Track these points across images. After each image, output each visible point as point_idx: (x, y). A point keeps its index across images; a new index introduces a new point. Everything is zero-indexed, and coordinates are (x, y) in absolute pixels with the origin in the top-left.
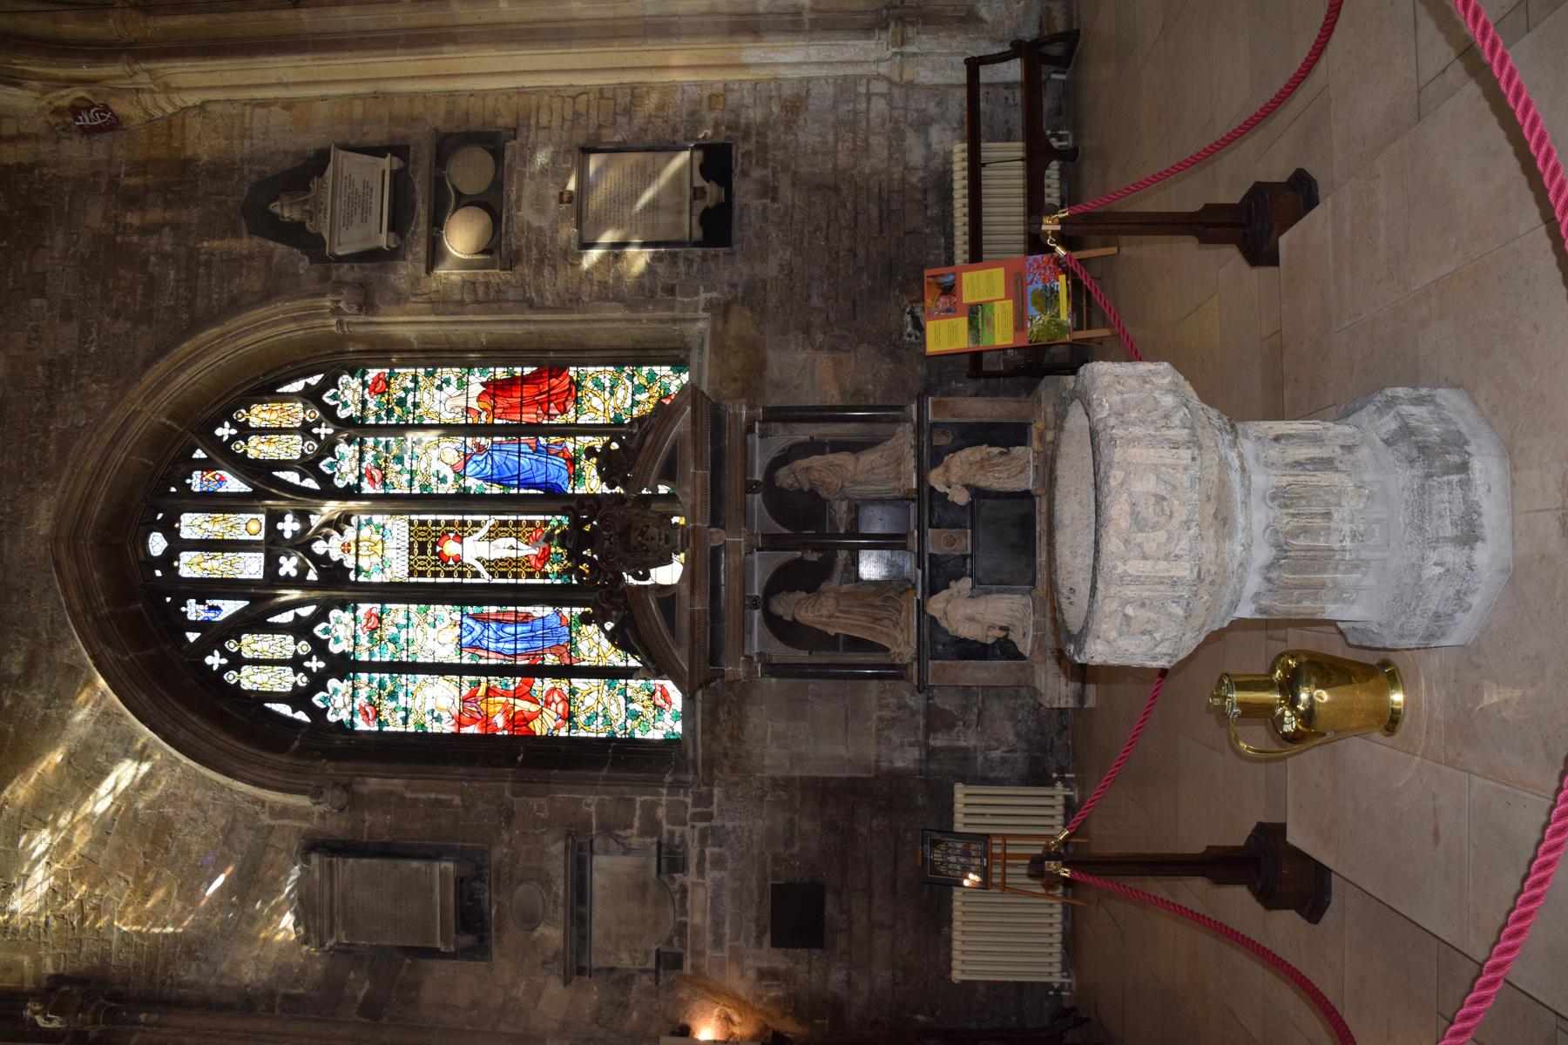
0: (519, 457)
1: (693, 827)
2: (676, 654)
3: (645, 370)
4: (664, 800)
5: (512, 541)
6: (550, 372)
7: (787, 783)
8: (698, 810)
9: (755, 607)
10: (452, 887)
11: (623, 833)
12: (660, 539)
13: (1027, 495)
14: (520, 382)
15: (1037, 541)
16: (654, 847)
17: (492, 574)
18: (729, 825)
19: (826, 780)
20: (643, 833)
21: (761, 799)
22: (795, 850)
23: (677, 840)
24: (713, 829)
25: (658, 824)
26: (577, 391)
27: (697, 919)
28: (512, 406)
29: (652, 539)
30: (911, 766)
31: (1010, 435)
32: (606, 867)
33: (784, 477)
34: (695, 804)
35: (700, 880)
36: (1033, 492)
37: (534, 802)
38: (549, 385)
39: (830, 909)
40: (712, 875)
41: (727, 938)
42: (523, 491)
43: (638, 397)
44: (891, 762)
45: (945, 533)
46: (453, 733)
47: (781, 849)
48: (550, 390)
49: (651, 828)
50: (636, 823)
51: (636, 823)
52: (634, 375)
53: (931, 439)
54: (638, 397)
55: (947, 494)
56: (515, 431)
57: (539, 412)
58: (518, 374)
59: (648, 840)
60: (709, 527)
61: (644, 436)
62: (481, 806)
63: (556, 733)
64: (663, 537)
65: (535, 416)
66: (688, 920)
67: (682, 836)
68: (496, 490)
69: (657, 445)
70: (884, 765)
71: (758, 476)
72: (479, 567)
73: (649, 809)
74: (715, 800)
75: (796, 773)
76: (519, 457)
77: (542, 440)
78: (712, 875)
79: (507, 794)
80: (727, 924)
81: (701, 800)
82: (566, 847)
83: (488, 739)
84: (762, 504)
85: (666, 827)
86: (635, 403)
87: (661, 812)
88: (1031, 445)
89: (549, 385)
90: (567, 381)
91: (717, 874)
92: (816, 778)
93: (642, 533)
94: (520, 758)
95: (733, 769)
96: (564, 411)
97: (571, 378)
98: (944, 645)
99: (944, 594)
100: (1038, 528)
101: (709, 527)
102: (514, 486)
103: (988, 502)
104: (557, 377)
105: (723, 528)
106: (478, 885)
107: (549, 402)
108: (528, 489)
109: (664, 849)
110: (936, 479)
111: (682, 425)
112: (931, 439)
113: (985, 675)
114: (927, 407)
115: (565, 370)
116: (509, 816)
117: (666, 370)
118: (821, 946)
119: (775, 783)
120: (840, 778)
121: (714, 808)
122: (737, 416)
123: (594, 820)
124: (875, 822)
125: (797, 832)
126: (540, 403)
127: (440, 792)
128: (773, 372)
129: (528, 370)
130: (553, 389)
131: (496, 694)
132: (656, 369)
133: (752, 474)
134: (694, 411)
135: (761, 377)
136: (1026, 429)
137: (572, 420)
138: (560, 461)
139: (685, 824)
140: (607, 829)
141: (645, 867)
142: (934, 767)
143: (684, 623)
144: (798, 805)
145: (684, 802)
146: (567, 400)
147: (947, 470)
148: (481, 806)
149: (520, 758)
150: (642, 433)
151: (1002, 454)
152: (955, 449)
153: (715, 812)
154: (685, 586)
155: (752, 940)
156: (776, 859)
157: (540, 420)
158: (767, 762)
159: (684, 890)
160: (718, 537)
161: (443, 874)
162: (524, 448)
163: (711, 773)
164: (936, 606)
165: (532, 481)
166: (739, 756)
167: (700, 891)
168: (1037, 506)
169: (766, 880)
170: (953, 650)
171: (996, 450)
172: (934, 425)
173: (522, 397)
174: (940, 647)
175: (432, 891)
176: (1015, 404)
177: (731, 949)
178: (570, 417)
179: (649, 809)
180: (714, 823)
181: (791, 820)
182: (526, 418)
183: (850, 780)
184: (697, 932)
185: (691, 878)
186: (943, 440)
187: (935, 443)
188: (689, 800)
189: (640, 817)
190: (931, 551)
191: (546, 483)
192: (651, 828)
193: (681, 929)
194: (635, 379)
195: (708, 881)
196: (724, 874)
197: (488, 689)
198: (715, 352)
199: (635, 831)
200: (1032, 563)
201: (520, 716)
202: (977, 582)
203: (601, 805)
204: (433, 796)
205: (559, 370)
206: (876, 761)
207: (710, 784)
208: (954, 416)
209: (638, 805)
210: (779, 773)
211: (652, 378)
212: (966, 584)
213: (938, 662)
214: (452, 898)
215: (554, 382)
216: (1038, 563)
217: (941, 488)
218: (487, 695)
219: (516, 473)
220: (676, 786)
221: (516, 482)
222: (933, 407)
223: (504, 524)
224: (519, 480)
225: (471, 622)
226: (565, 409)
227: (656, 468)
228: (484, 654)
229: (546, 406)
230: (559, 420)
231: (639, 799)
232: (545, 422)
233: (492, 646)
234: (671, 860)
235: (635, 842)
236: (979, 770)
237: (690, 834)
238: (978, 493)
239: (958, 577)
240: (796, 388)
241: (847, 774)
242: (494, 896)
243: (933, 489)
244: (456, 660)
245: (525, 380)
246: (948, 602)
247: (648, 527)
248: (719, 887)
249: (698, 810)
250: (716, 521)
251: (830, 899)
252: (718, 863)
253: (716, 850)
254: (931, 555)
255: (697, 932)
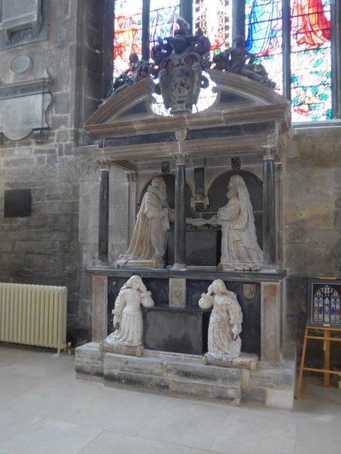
0: (269, 21)
1: (56, 146)
2: (113, 118)
3: (329, 92)
4: (69, 129)
5: (217, 27)
6: (327, 29)
7: (76, 195)
8: (64, 147)
9: (163, 170)
10: (26, 23)
11: (53, 109)
12: (180, 97)
13: (205, 349)
14: (320, 10)
15: (173, 353)
16: (46, 126)
17: (198, 19)
18: (57, 165)
19: (77, 216)
20: (53, 119)
21: (69, 181)
22: (45, 201)
23: (51, 138)
24: (55, 157)
25: (57, 127)
26: (313, 49)
27: (17, 152)
28: (302, 9)
29: (180, 92)
30: (84, 263)
31: (251, 341)
32: (36, 102)
33: (237, 181)
34: (66, 145)
35: (33, 152)
36: (206, 354)
37: (67, 59)
38: (318, 30)
39: (21, 220)
40: (34, 157)
41: (9, 168)
42: (247, 27)
43: (309, 90)
44: (85, 252)
45: (184, 289)
46: (114, 15)
47: (46, 193)
48: (313, 31)
49: (58, 123)
50: (58, 115)
51: (58, 115)
52: (324, 85)
53: (248, 283)
54: (309, 90)
55: (206, 292)
56: (287, 17)
57: (299, 28)
58: (325, 9)
59: (50, 122)
60: (187, 129)
61: (250, 76)
62: (65, 30)
63: (115, 70)
64: (182, 99)
65: (296, 25)
66: (16, 147)
67: (53, 141)
68: (248, 11)
69: (243, 87)
70: (84, 248)
71: (243, 167)
72: (202, 10)
73: (63, 121)
74: (68, 156)
75: (81, 200)
76: (269, 21)
77: (280, 33)
78: (34, 157)
79: (71, 43)
80: (14, 168)
81: (68, 147)
82: (44, 79)
83: (111, 34)
84: (223, 172)
85: (56, 131)
86: (305, 89)
87: (63, 128)
88: (240, 356)
89: (318, 30)
90: (320, 42)
91: (35, 160)
92: (78, 210)
93: (183, 85)
94: (97, 51)
95: (83, 165)
96: (299, 43)
97: (323, 44)
98: (116, 286)
99: (143, 287)
100: (181, 354)
101: (187, 129)
102: (250, 21)
103: (200, 322)
104: (324, 34)
105: (187, 139)
106: (30, 36)
107: (306, 33)
108: (249, 30)
109: (45, 131)
110: (217, 285)
111: (259, 101)
112: (248, 283)
113: (99, 310)
114: (271, 281)
115: (328, 39)
116: (61, 47)
117: (328, 105)
118: (6, 216)
119: (76, 188)
120: (78, 224)
121: (64, 156)
122: (265, 141)
123: (59, 92)
124: (58, 243)
125: (54, 201)
126: (305, 27)
127: (71, 7)
128: (319, 173)
129: (328, 16)
130: (315, 33)
131: (134, 36)
132: (330, 99)
133: (245, 162)
134: (267, 108)
135: (316, 165)
136: (255, 353)
137: (293, 50)
138: (266, 47)
139: (57, 142)
140: (54, 101)
141: (37, 122)
142: (83, 276)
143: (132, 119)
144: (66, 201)
145: (67, 140)
146: (307, 44)
147: (224, 294)
148: (65, 30)
149: (97, 51)
150: (253, 74)
151: (233, 335)
152: (240, 300)
153: (63, 157)
154: (152, 117)
155: (7, 181)
156: (42, 191)
157: (293, 29)
158: (86, 183)
159: (29, 144)
160: (180, 135)
161: (31, 17)
162: (274, 23)
163: (81, 153)
164: (135, 281)
165: (253, 31)
166: (89, 168)
167: (28, 153)
168: (197, 356)
169: (33, 186)
170: (113, 291)
171: (236, 330)
172: (258, 285)
173: (309, 14)
174: (114, 283)
175: (25, 12)
176: (274, 346)
177: (5, 171)
178: (295, 47)
179: (63, 121)
180: (58, 158)
181: (59, 198)
182: (294, 21)
183: (78, 229)
184: (11, 152)
185: (35, 147)
186: (247, 291)
187: (245, 285)
188: (68, 142)
189: (61, 117)
190: (171, 280)
191: (252, 40)
192: (58, 123)
193: (13, 143)
194: (323, 86)
195: (32, 156)
196: (36, 163)
197: (136, 30)
198: (333, 132)
199: (54, 115)
200: (159, 348)
201: (122, 48)
202: (150, 310)
203: (67, 95)
204: (70, 4)
205: (328, 34)
206: (86, 244)
207: (76, 154)
208: (265, 301)
209: (65, 115)
210: (81, 190)
211: (322, 97)
212: (148, 302)
213: (106, 281)
214: (21, 23)
215: (320, 33)
216: (160, 352)
217: (210, 289)
218: (133, 30)
219: (259, 20)
220: (77, 136)
221: (252, 22)
222: (271, 286)
223: (227, 20)
224: (254, 23)
225: (171, 13)
226: (301, 44)
227: (229, 89)
228: (155, 23)
229: (303, 31)
230: (293, 42)
231: (69, 115)
232: (292, 33)
233: (158, 28)
234: (41, 135)
235: (50, 116)
236: (83, 301)
237: (53, 145)
238: (206, 315)
239: (154, 297)
240: (307, 190)
241: (80, 227)
242: (26, 47)
243: (210, 282)
244: (151, 9)
245: (320, 13)
246: (138, 290)
247: (188, 88)
248: (28, 161)
249: (64, 147)
250: (192, 135)
251: (25, 219)
252: (40, 160)
253: (46, 159)
254: (167, 280)
255: (11, 152)
